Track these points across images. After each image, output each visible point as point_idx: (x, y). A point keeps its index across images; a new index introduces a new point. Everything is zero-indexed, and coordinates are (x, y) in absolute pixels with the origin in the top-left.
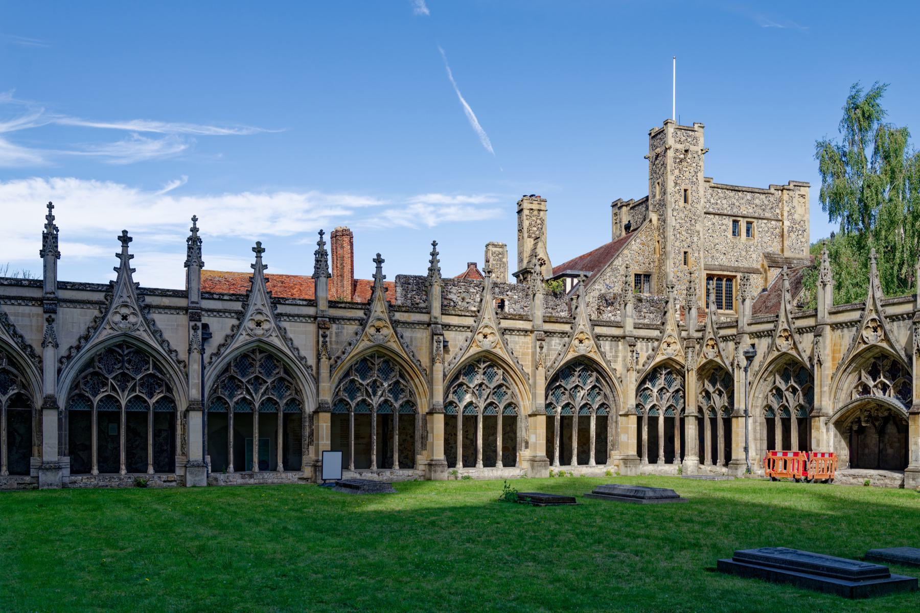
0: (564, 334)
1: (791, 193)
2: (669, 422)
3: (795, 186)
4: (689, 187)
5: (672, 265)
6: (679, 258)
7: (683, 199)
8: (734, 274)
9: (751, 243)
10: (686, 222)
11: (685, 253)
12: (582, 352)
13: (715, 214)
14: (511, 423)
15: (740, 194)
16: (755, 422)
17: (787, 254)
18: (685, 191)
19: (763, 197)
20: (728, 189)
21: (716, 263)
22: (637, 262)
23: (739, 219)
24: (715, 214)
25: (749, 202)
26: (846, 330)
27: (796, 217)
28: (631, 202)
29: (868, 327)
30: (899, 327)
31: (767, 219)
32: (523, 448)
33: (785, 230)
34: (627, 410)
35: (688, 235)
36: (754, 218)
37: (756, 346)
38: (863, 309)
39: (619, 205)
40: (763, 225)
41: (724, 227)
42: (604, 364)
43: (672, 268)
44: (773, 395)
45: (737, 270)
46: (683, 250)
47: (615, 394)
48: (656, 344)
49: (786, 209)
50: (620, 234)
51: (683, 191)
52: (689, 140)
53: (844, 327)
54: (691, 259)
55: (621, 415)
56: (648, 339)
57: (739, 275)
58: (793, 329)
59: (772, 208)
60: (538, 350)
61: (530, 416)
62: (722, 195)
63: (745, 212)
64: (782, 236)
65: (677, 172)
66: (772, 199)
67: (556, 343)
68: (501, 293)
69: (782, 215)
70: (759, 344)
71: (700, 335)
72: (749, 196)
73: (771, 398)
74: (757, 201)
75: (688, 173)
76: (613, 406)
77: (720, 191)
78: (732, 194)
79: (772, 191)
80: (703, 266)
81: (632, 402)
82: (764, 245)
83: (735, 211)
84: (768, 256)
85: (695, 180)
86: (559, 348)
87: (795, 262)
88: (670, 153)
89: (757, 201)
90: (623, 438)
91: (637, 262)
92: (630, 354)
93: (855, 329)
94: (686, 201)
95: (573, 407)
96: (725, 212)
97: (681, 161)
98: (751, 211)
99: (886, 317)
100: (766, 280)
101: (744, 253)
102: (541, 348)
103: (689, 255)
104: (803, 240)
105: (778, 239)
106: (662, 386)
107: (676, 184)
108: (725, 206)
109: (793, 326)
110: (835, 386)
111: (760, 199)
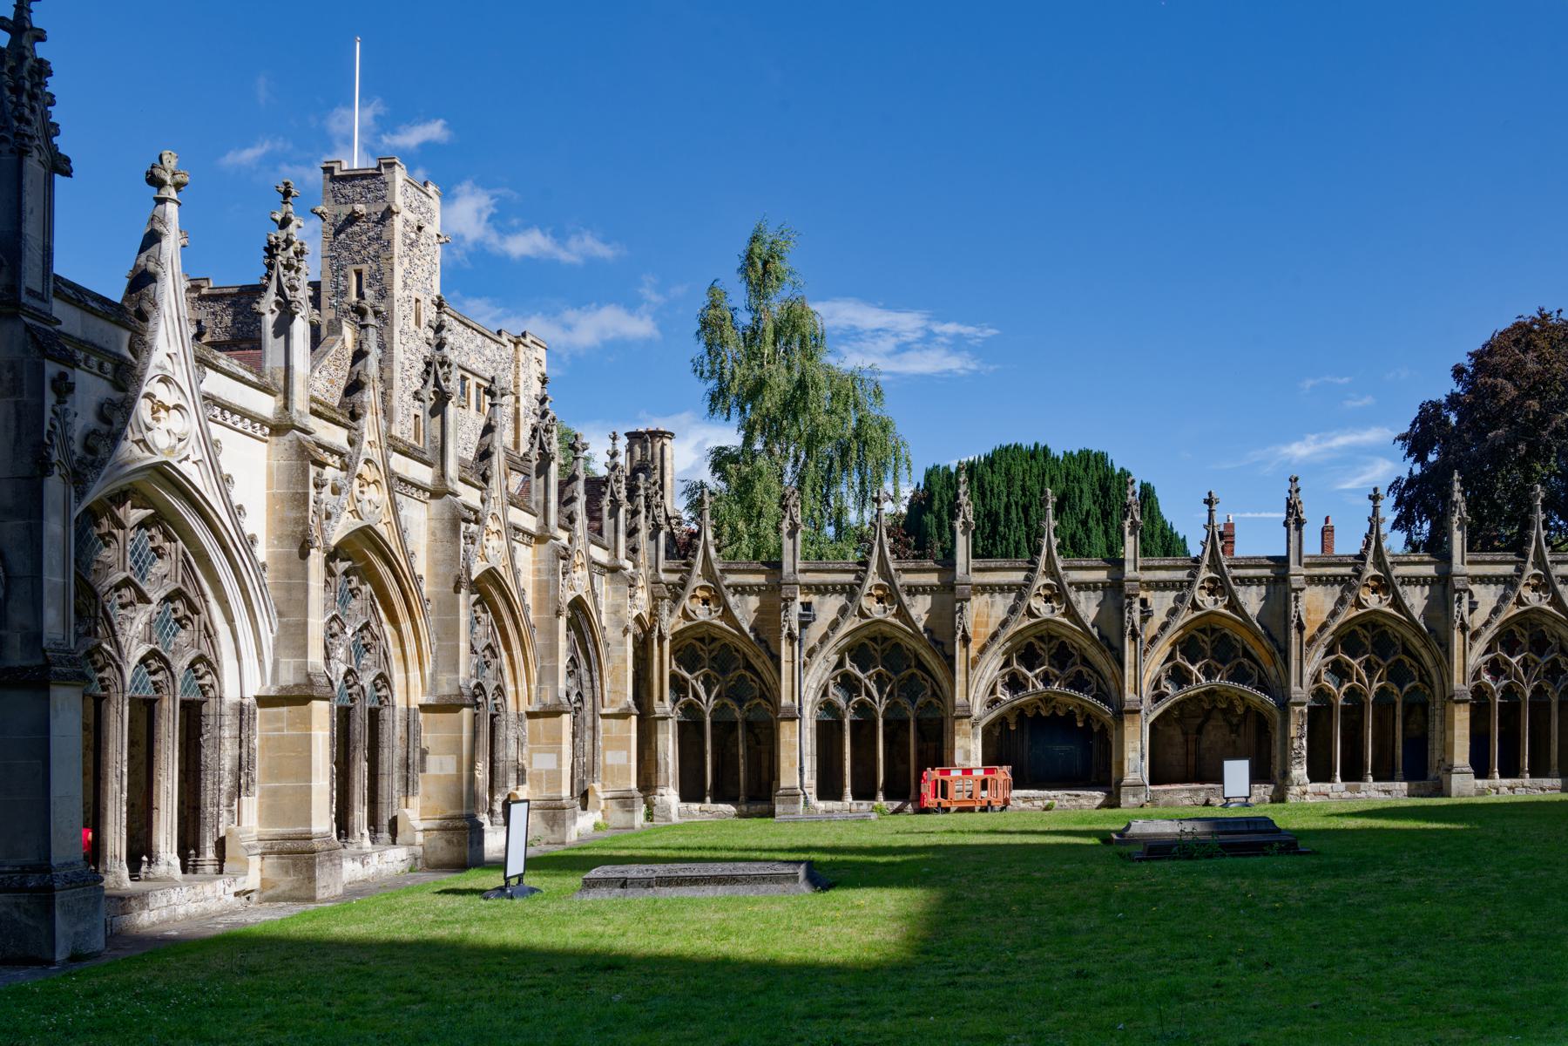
1: (528, 352)
3: (532, 342)
6: (408, 425)
7: (413, 314)
19: (494, 346)
20: (456, 319)
23: (468, 375)
25: (479, 350)
26: (998, 597)
28: (204, 284)
29: (1040, 595)
30: (1087, 599)
37: (814, 605)
38: (1033, 570)
47: (596, 675)
53: (994, 591)
55: (605, 716)
58: (898, 587)
61: (531, 715)
63: (474, 366)
69: (517, 386)
70: (821, 604)
75: (420, 269)
79: (504, 339)
85: (429, 287)
88: (398, 222)
93: (1013, 595)
99: (1070, 584)
107: (405, 284)
109: (898, 583)
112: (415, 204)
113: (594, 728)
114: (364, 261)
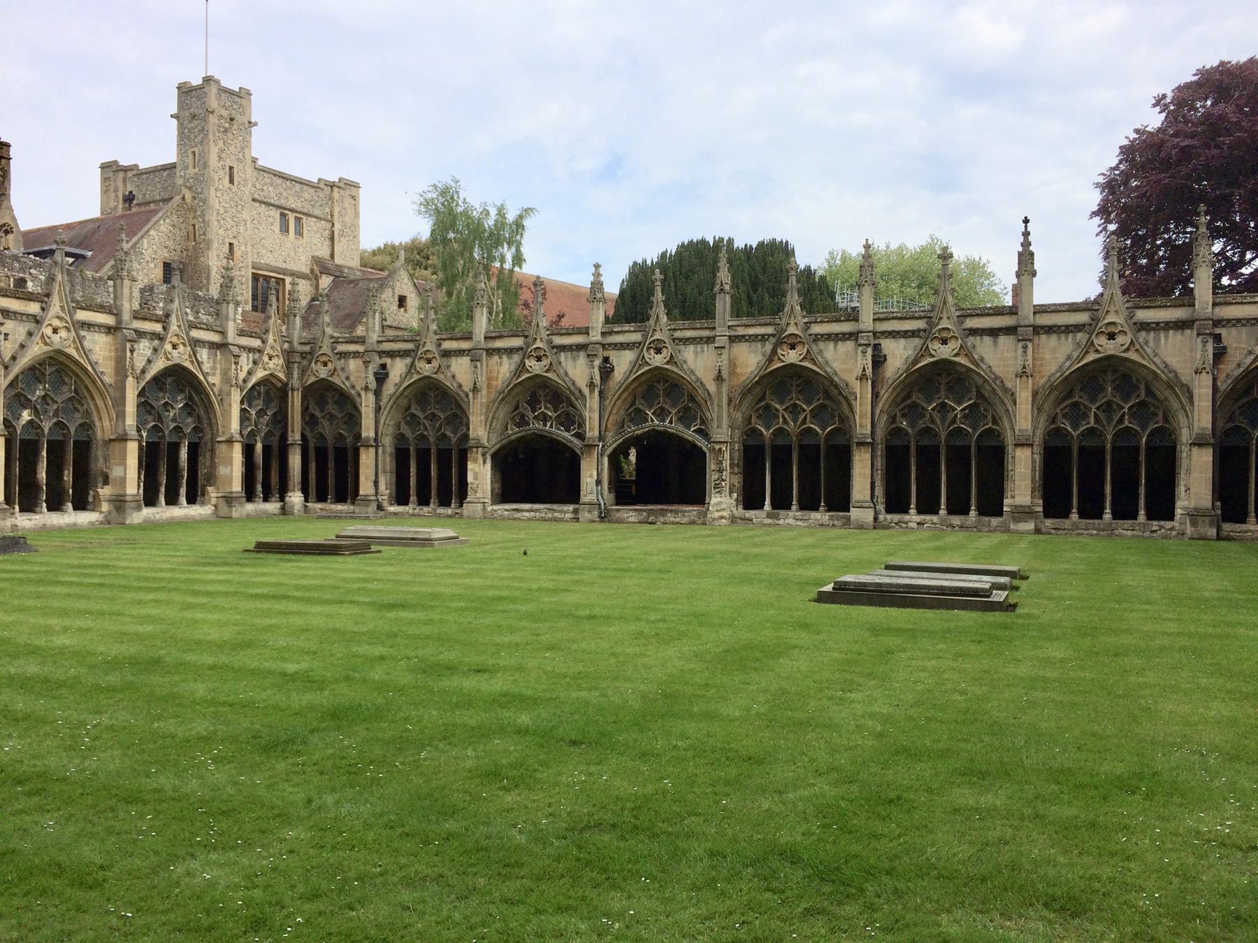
0: (155, 336)
1: (342, 192)
2: (266, 449)
4: (234, 164)
5: (216, 258)
6: (224, 250)
8: (281, 276)
9: (300, 242)
10: (231, 207)
11: (231, 244)
12: (176, 361)
13: (261, 202)
14: (84, 449)
15: (288, 182)
16: (384, 452)
17: (338, 261)
18: (231, 168)
19: (312, 190)
21: (263, 262)
22: (166, 247)
23: (287, 212)
24: (261, 202)
27: (347, 219)
31: (317, 217)
32: (100, 485)
33: (336, 234)
34: (229, 436)
35: (233, 224)
36: (304, 214)
39: (114, 168)
40: (312, 224)
41: (270, 220)
42: (201, 378)
43: (214, 261)
44: (407, 423)
45: (284, 271)
46: (228, 241)
47: (212, 416)
48: (257, 355)
49: (337, 209)
50: (116, 207)
51: (228, 169)
52: (235, 107)
54: (237, 253)
56: (250, 350)
57: (288, 280)
59: (321, 206)
60: (128, 354)
62: (268, 181)
63: (293, 206)
64: (332, 239)
65: (220, 143)
66: (321, 195)
67: (144, 347)
68: (22, 270)
69: (332, 216)
71: (307, 348)
72: (298, 186)
73: (403, 426)
74: (306, 195)
76: (208, 431)
77: (266, 175)
78: (279, 181)
79: (322, 185)
80: (250, 264)
81: (235, 425)
82: (314, 247)
83: (282, 202)
84: (317, 261)
86: (149, 353)
87: (346, 271)
89: (306, 195)
90: (222, 470)
91: (166, 247)
92: (233, 366)
94: (231, 181)
95: (162, 431)
96: (272, 201)
97: (226, 131)
98: (299, 204)
100: (317, 287)
101: (292, 254)
102: (132, 351)
103: (236, 249)
104: (354, 247)
105: (328, 242)
106: (260, 407)
107: (220, 157)
108: (273, 195)
110: (491, 416)
111: (308, 193)
112: (228, 104)
113: (213, 451)
114: (196, 146)
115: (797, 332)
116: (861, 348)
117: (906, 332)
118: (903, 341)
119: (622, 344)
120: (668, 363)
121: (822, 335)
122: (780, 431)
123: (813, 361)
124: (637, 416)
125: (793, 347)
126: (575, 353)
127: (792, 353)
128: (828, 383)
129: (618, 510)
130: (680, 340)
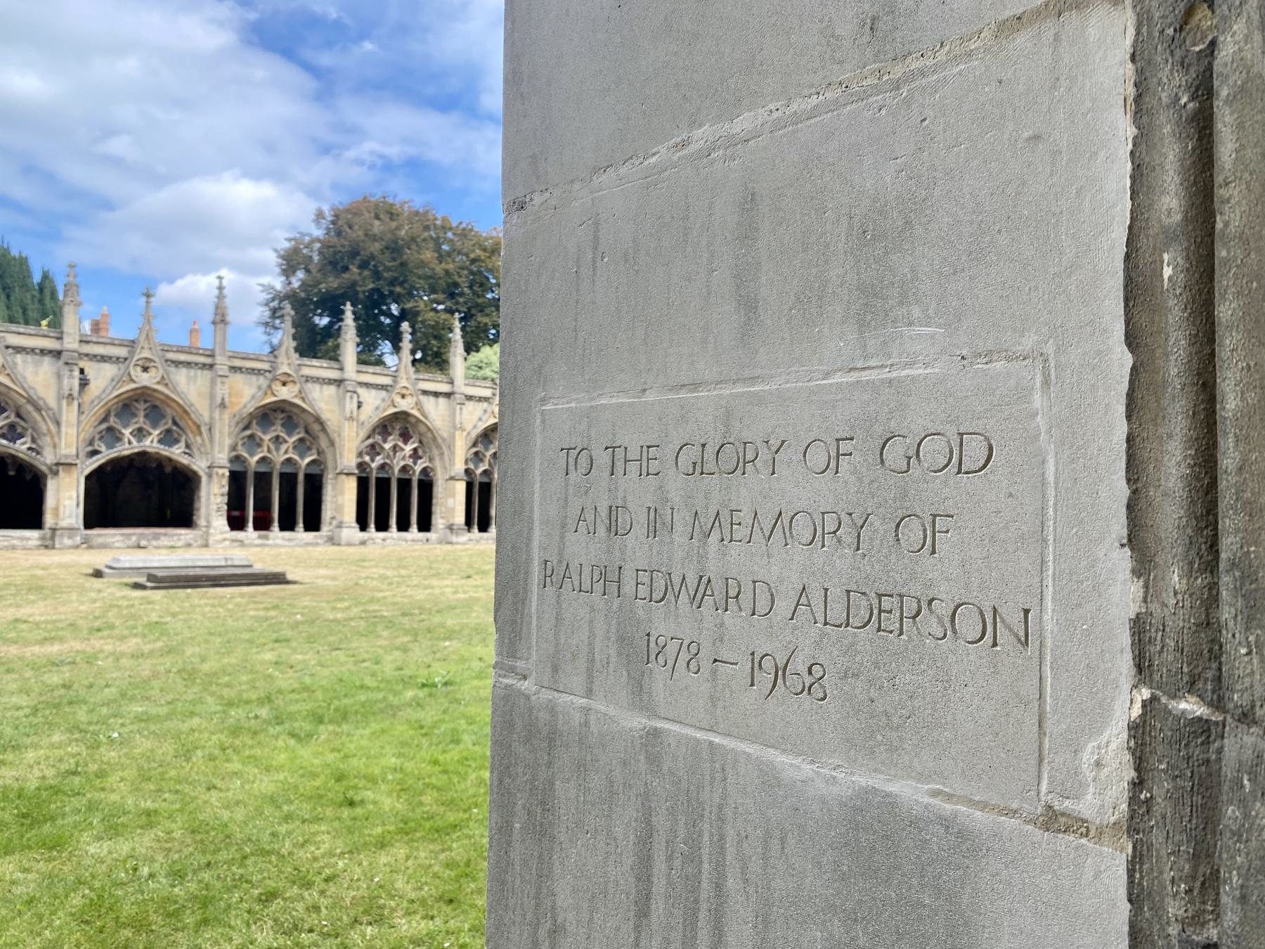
115: (289, 372)
116: (349, 394)
117: (377, 385)
118: (373, 392)
119: (102, 357)
120: (158, 383)
121: (312, 378)
122: (263, 459)
123: (303, 399)
124: (112, 435)
125: (284, 384)
126: (37, 357)
127: (284, 389)
128: (311, 420)
129: (100, 535)
130: (173, 362)
